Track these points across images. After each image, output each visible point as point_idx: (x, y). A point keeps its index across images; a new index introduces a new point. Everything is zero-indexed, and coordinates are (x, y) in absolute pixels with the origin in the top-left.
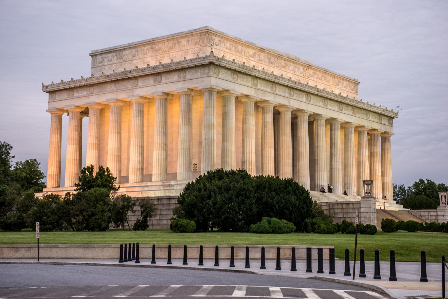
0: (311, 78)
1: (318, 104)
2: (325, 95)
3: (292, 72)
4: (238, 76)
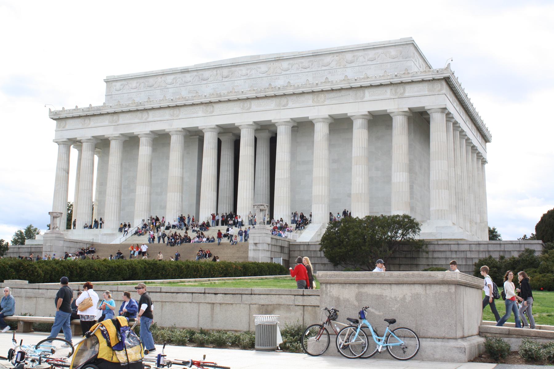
0: (284, 73)
1: (231, 112)
2: (235, 97)
3: (245, 77)
4: (90, 120)
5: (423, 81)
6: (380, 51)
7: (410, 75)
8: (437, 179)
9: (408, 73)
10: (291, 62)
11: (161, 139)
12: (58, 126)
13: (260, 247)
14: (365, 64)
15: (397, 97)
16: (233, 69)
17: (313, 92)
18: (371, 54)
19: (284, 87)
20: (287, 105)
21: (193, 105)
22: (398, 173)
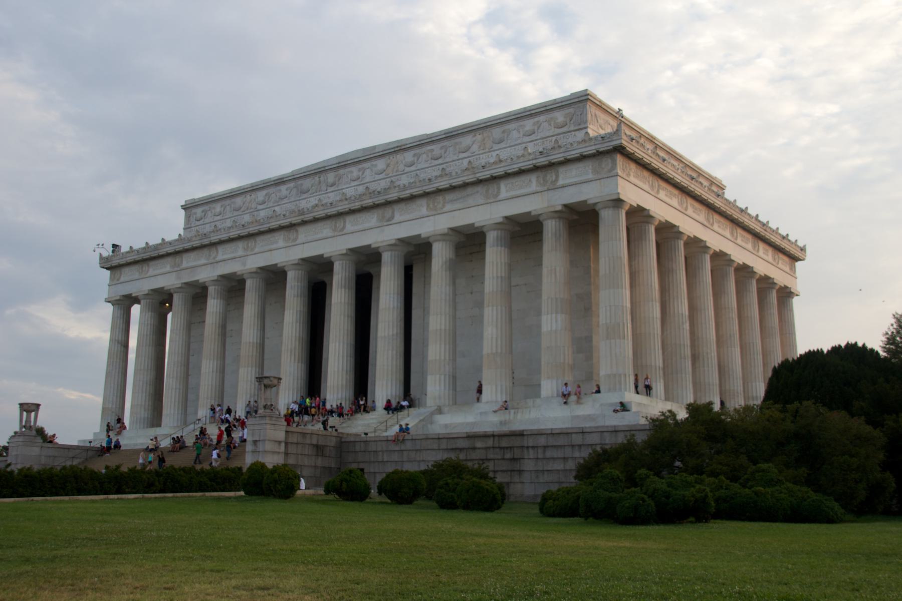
0: (407, 169)
1: (319, 236)
3: (356, 183)
5: (582, 158)
6: (542, 118)
7: (562, 150)
8: (608, 321)
9: (560, 147)
10: (417, 151)
11: (234, 287)
12: (112, 279)
13: (261, 447)
14: (519, 141)
15: (546, 188)
16: (341, 171)
17: (426, 195)
18: (529, 124)
19: (386, 190)
20: (392, 217)
21: (271, 231)
22: (549, 316)
